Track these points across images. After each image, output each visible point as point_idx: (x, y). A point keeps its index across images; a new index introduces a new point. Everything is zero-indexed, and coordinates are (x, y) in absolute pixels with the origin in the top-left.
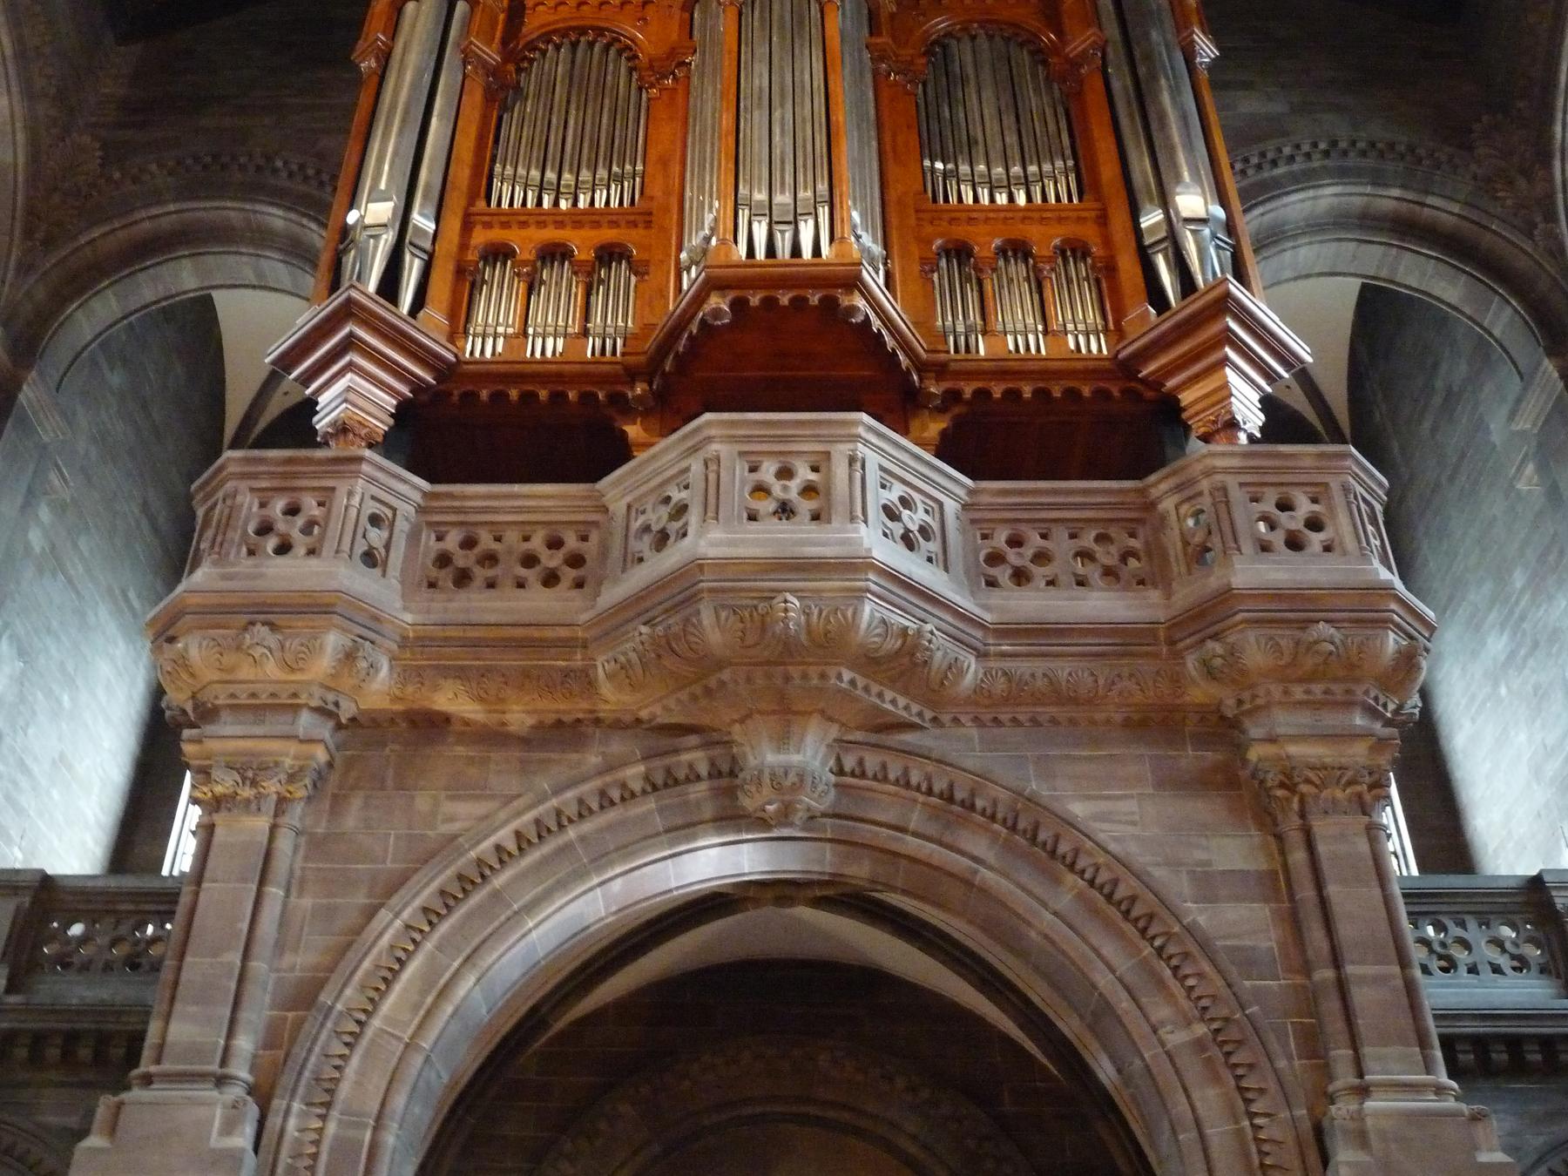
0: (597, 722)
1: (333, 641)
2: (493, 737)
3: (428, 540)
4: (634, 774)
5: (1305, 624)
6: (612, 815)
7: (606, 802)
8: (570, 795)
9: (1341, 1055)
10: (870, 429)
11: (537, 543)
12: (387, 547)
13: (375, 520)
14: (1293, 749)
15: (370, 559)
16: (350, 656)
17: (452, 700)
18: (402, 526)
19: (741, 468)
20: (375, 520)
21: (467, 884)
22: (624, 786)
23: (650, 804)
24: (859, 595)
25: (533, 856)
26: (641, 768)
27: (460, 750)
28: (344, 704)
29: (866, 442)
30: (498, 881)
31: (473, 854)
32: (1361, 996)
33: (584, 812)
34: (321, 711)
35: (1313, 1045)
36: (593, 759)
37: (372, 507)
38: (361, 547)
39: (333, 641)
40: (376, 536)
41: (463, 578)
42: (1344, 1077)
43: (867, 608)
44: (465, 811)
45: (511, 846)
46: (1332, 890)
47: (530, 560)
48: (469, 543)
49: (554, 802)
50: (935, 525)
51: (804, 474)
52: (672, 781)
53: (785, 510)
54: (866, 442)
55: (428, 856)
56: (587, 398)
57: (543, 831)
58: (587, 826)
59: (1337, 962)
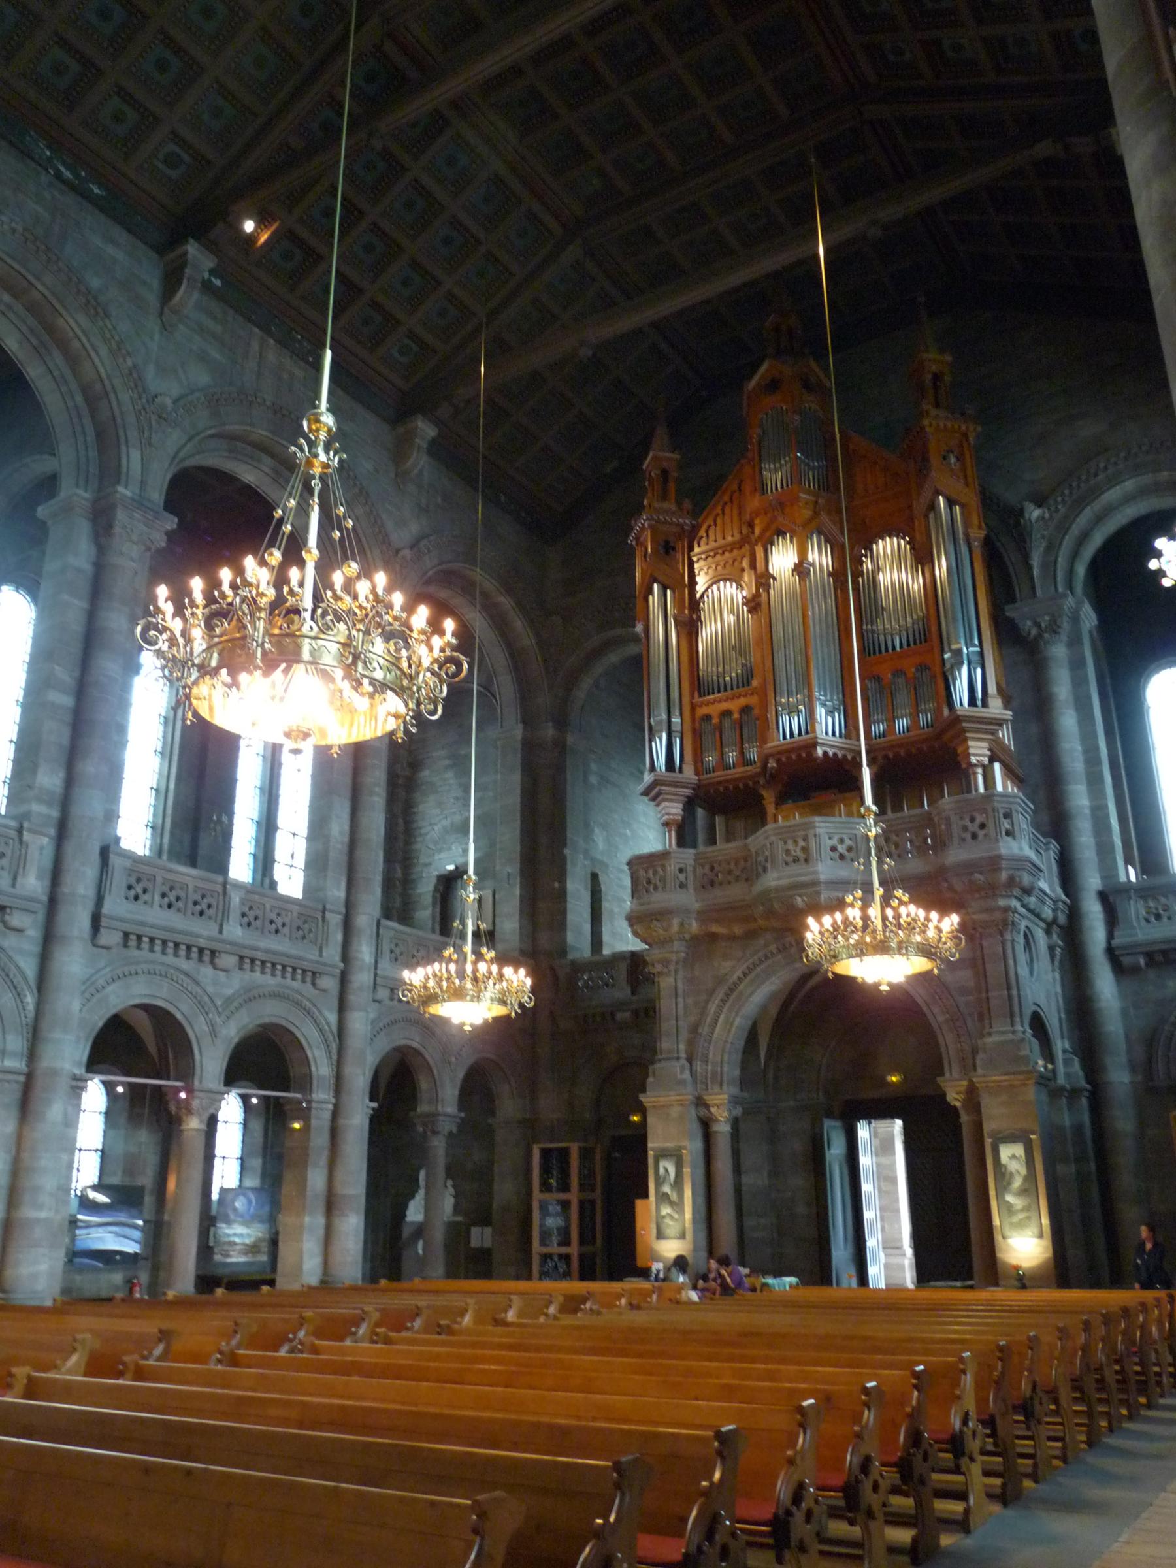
0: (761, 929)
1: (676, 922)
2: (732, 938)
3: (700, 870)
4: (773, 947)
5: (972, 874)
6: (770, 962)
7: (767, 957)
8: (755, 957)
9: (987, 1021)
10: (819, 822)
11: (732, 866)
12: (686, 879)
13: (681, 870)
14: (975, 917)
15: (682, 886)
16: (682, 925)
17: (715, 928)
18: (690, 869)
19: (781, 844)
20: (681, 870)
21: (732, 990)
22: (771, 952)
23: (780, 956)
24: (818, 893)
25: (748, 978)
26: (775, 946)
27: (723, 944)
28: (686, 935)
29: (819, 827)
30: (741, 987)
31: (731, 981)
32: (993, 1002)
33: (761, 961)
34: (680, 940)
35: (981, 1017)
36: (762, 942)
37: (678, 866)
38: (678, 883)
39: (676, 922)
40: (682, 877)
41: (712, 884)
42: (987, 1027)
43: (822, 896)
44: (727, 965)
45: (742, 976)
46: (988, 966)
47: (730, 872)
48: (712, 868)
49: (751, 961)
50: (854, 846)
51: (802, 843)
52: (785, 948)
53: (796, 860)
54: (819, 827)
55: (719, 981)
56: (746, 785)
57: (750, 970)
58: (762, 966)
59: (987, 991)
